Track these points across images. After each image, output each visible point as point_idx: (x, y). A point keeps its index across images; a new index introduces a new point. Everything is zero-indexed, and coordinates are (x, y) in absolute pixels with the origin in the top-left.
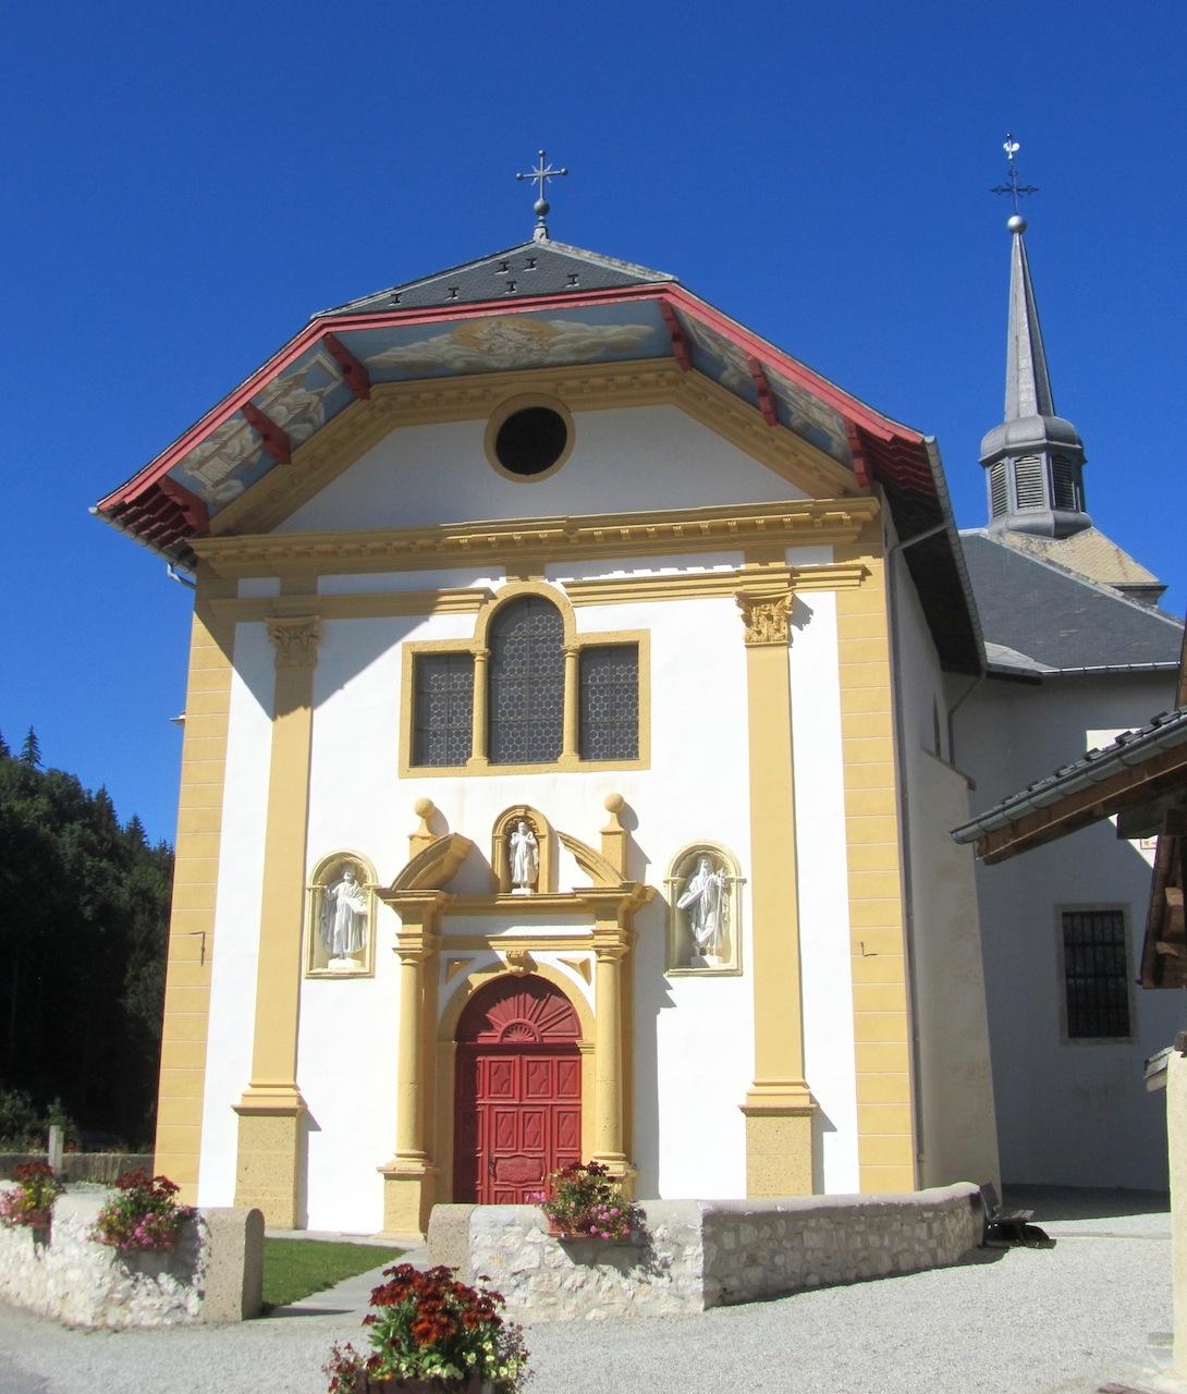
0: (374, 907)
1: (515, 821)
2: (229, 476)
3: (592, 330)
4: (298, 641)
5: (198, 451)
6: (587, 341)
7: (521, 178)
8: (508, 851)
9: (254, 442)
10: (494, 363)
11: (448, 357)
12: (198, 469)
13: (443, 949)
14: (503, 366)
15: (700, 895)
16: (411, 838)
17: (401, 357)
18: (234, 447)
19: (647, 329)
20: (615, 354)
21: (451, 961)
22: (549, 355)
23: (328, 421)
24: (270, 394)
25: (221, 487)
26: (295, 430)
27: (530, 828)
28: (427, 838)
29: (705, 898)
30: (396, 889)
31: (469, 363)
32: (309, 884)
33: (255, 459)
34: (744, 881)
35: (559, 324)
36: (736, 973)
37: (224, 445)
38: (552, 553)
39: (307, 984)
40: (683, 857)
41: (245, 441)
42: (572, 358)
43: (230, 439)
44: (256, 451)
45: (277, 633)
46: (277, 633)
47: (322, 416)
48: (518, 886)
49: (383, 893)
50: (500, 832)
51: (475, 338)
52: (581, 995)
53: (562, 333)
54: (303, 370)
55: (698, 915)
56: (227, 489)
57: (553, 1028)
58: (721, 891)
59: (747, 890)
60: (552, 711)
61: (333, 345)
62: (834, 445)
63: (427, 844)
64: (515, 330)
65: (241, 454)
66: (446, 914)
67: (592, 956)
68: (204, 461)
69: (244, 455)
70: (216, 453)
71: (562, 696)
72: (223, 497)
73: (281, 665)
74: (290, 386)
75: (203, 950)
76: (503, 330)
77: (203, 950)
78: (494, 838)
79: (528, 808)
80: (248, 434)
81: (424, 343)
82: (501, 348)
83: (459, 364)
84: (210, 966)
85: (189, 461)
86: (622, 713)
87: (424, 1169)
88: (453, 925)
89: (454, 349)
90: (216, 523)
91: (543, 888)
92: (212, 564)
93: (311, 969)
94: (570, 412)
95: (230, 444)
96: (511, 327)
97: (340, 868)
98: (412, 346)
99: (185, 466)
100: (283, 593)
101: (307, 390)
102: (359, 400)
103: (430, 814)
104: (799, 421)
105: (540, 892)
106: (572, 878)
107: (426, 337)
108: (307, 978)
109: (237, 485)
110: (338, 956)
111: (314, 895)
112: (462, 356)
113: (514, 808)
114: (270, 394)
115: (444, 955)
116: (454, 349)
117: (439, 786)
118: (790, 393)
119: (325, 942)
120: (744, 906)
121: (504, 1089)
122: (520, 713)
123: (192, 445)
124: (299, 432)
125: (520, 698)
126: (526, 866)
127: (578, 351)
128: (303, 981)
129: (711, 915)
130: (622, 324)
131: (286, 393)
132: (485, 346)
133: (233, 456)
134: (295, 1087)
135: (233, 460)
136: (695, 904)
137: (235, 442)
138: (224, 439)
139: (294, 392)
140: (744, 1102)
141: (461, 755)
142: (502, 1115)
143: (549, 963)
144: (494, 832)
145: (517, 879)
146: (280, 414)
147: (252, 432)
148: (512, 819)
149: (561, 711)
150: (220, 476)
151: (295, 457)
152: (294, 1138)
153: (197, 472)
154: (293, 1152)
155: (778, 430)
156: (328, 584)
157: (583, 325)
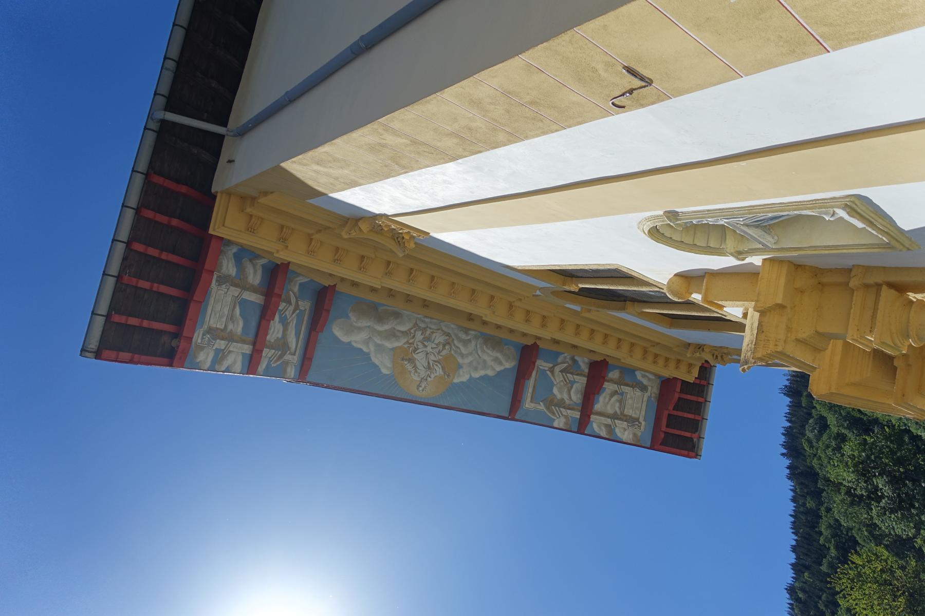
3: (370, 349)
6: (386, 327)
12: (638, 420)
17: (496, 360)
20: (375, 312)
24: (566, 417)
25: (645, 382)
26: (584, 362)
33: (614, 375)
37: (614, 417)
41: (604, 402)
43: (608, 416)
51: (443, 368)
53: (392, 349)
54: (542, 407)
65: (616, 393)
68: (632, 421)
69: (614, 387)
74: (555, 406)
76: (423, 373)
85: (635, 435)
98: (482, 373)
99: (639, 434)
101: (551, 385)
112: (466, 343)
114: (566, 417)
116: (462, 356)
127: (397, 315)
130: (350, 342)
131: (561, 404)
133: (621, 397)
135: (622, 394)
137: (610, 411)
138: (609, 421)
139: (559, 396)
147: (598, 401)
150: (638, 393)
153: (641, 420)
157: (373, 359)
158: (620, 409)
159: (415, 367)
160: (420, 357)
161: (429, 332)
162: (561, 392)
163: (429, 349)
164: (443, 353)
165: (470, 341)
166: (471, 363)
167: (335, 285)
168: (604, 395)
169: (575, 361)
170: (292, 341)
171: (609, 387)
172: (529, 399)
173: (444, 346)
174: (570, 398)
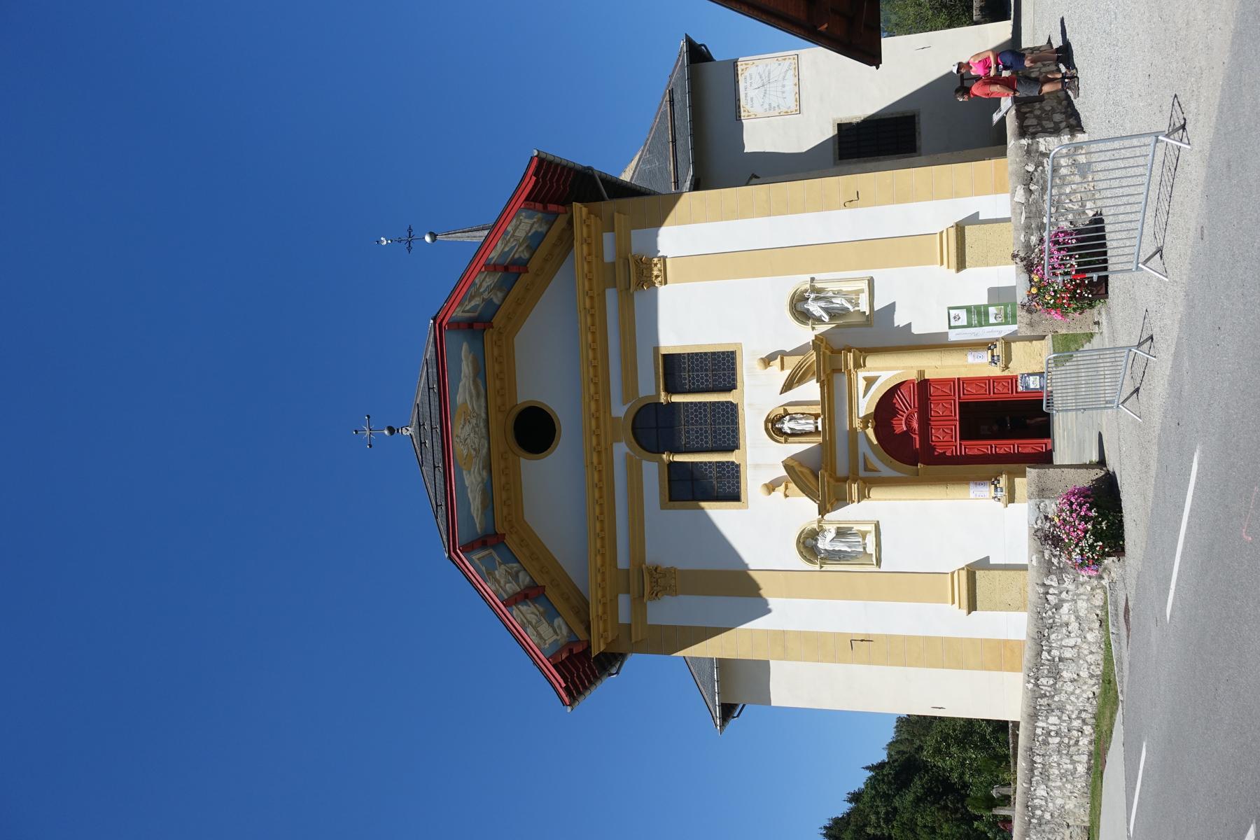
0: (831, 522)
1: (774, 427)
2: (551, 624)
3: (464, 380)
4: (659, 580)
5: (533, 638)
6: (472, 388)
7: (370, 446)
8: (794, 434)
9: (530, 606)
10: (485, 451)
11: (479, 479)
13: (858, 475)
14: (486, 445)
15: (821, 307)
16: (786, 496)
17: (478, 510)
18: (533, 619)
19: (465, 346)
20: (480, 372)
21: (866, 469)
22: (480, 415)
23: (519, 562)
26: (523, 582)
27: (780, 419)
28: (786, 488)
29: (823, 304)
30: (818, 500)
31: (483, 468)
32: (817, 567)
33: (541, 609)
34: (813, 279)
35: (459, 399)
36: (871, 282)
37: (530, 623)
38: (605, 412)
39: (884, 567)
40: (797, 319)
42: (483, 400)
43: (526, 618)
44: (535, 607)
45: (654, 594)
46: (654, 594)
47: (515, 565)
48: (817, 427)
49: (823, 511)
50: (782, 439)
51: (467, 455)
52: (886, 381)
53: (466, 400)
55: (833, 309)
56: (560, 627)
57: (909, 401)
58: (819, 294)
59: (817, 276)
60: (705, 410)
61: (468, 548)
62: (540, 230)
63: (792, 486)
64: (462, 428)
65: (537, 616)
66: (835, 473)
67: (862, 374)
68: (539, 635)
69: (538, 613)
70: (535, 628)
71: (695, 404)
72: (565, 631)
73: (672, 591)
74: (493, 577)
75: (862, 640)
77: (862, 640)
78: (786, 442)
79: (767, 421)
80: (524, 608)
81: (469, 490)
82: (474, 443)
83: (485, 474)
84: (873, 635)
86: (706, 365)
87: (1004, 476)
88: (842, 468)
89: (474, 472)
90: (582, 636)
91: (818, 409)
92: (610, 640)
93: (873, 564)
94: (517, 404)
95: (530, 620)
96: (460, 431)
97: (808, 544)
98: (471, 501)
100: (628, 592)
102: (505, 541)
103: (771, 487)
104: (525, 253)
105: (819, 411)
106: (811, 390)
107: (464, 488)
108: (880, 567)
109: (558, 622)
110: (864, 548)
111: (825, 564)
113: (767, 429)
115: (862, 473)
116: (474, 472)
117: (752, 483)
118: (506, 249)
119: (856, 557)
120: (830, 280)
121: (949, 432)
122: (706, 432)
123: (528, 640)
124: (524, 579)
125: (697, 432)
126: (803, 421)
127: (478, 395)
128: (882, 569)
129: (834, 300)
131: (499, 583)
132: (473, 453)
134: (953, 573)
136: (826, 310)
137: (528, 616)
138: (525, 621)
139: (497, 576)
140: (953, 270)
141: (733, 469)
142: (965, 391)
143: (866, 404)
144: (781, 443)
145: (811, 428)
146: (512, 588)
147: (522, 606)
148: (774, 432)
149: (705, 404)
150: (551, 630)
151: (540, 582)
152: (987, 572)
154: (996, 572)
155: (533, 266)
156: (623, 562)
157: (461, 384)
158: (536, 623)
159: (464, 426)
160: (468, 428)
161: (477, 429)
162: (500, 576)
163: (472, 435)
164: (472, 451)
165: (480, 474)
166: (472, 483)
167: (492, 327)
168: (528, 608)
169: (517, 573)
170: (473, 303)
171: (532, 609)
172: (478, 556)
173: (475, 450)
174: (505, 586)
